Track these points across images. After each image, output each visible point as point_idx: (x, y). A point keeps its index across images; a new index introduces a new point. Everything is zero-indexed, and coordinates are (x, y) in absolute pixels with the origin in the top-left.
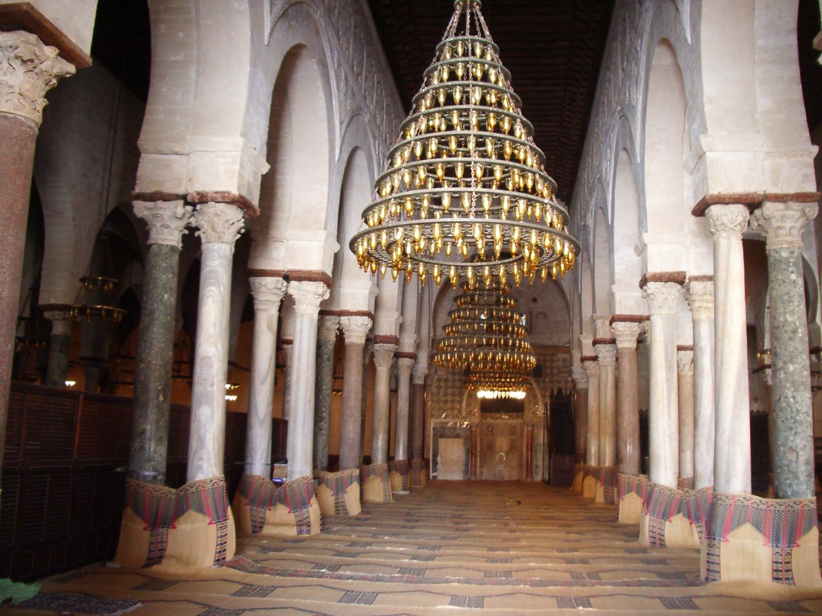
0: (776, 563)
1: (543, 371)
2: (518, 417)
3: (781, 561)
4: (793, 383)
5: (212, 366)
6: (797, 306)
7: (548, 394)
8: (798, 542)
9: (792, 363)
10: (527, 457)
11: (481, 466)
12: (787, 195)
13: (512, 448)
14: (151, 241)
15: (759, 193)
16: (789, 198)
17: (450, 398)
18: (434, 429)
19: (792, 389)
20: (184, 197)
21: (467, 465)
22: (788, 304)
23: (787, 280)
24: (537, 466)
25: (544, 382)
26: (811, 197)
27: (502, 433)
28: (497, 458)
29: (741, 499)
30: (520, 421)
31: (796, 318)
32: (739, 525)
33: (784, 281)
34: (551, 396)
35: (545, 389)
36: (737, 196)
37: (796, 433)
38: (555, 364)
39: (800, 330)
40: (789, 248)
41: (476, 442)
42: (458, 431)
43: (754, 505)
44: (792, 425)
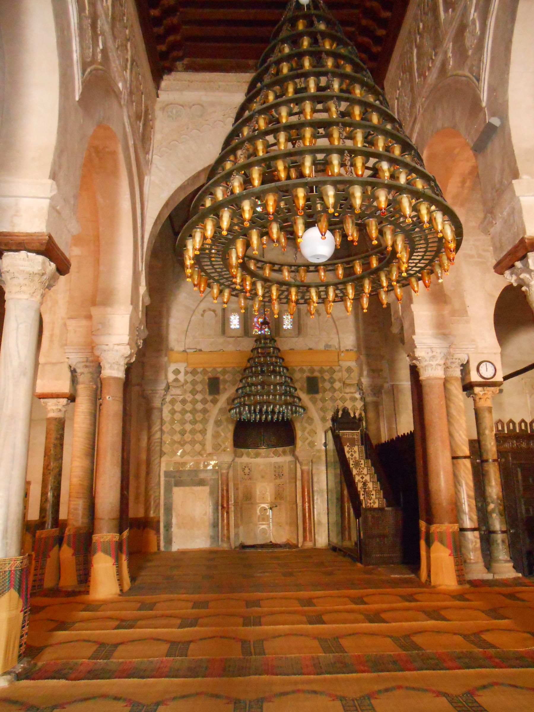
1: (320, 385)
2: (284, 453)
7: (330, 415)
10: (304, 509)
11: (237, 526)
13: (279, 496)
17: (188, 427)
18: (167, 474)
21: (215, 525)
24: (320, 523)
25: (323, 400)
27: (263, 477)
30: (289, 458)
34: (334, 419)
35: (323, 409)
38: (336, 376)
41: (227, 491)
42: (202, 476)
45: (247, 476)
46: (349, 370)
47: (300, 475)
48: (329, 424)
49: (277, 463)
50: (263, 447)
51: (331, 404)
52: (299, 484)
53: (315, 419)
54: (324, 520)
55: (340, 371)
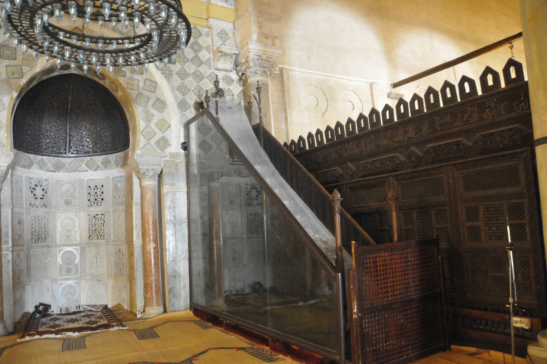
2: (106, 164)
13: (95, 233)
24: (176, 275)
27: (68, 203)
28: (59, 259)
30: (117, 172)
35: (183, 90)
45: (39, 200)
46: (223, 34)
47: (139, 196)
48: (191, 113)
49: (93, 180)
50: (70, 155)
51: (195, 84)
52: (136, 211)
53: (168, 102)
54: (183, 268)
55: (207, 35)
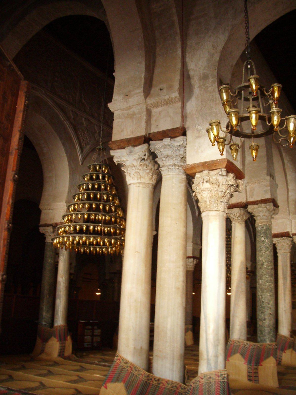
0: (249, 372)
3: (251, 371)
4: (261, 289)
5: (60, 285)
6: (264, 253)
8: (262, 363)
9: (261, 280)
12: (257, 201)
14: (46, 241)
15: (243, 202)
16: (258, 202)
19: (261, 292)
20: (51, 225)
22: (260, 252)
23: (260, 241)
26: (268, 201)
29: (236, 342)
31: (263, 258)
32: (234, 354)
33: (259, 241)
36: (233, 205)
37: (262, 312)
39: (265, 264)
40: (261, 226)
43: (244, 345)
44: (260, 309)
